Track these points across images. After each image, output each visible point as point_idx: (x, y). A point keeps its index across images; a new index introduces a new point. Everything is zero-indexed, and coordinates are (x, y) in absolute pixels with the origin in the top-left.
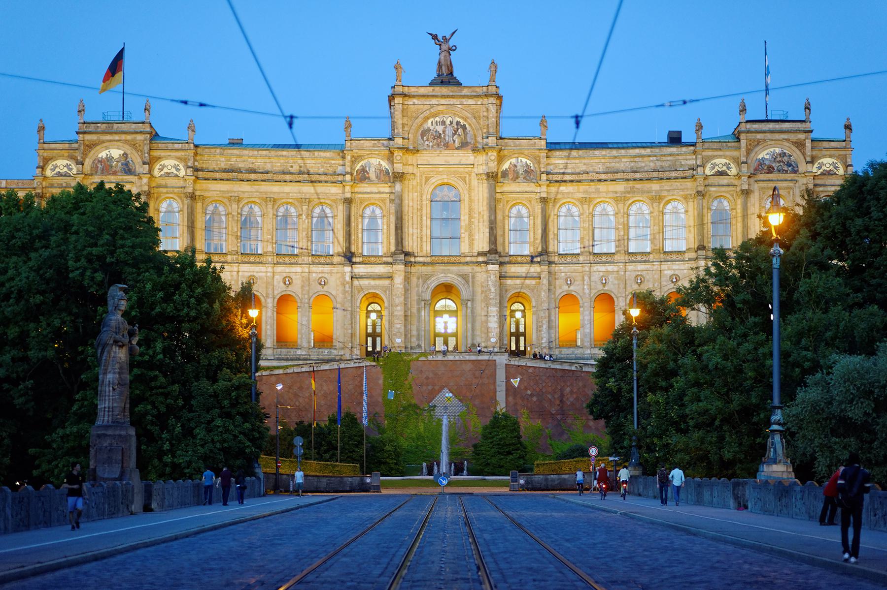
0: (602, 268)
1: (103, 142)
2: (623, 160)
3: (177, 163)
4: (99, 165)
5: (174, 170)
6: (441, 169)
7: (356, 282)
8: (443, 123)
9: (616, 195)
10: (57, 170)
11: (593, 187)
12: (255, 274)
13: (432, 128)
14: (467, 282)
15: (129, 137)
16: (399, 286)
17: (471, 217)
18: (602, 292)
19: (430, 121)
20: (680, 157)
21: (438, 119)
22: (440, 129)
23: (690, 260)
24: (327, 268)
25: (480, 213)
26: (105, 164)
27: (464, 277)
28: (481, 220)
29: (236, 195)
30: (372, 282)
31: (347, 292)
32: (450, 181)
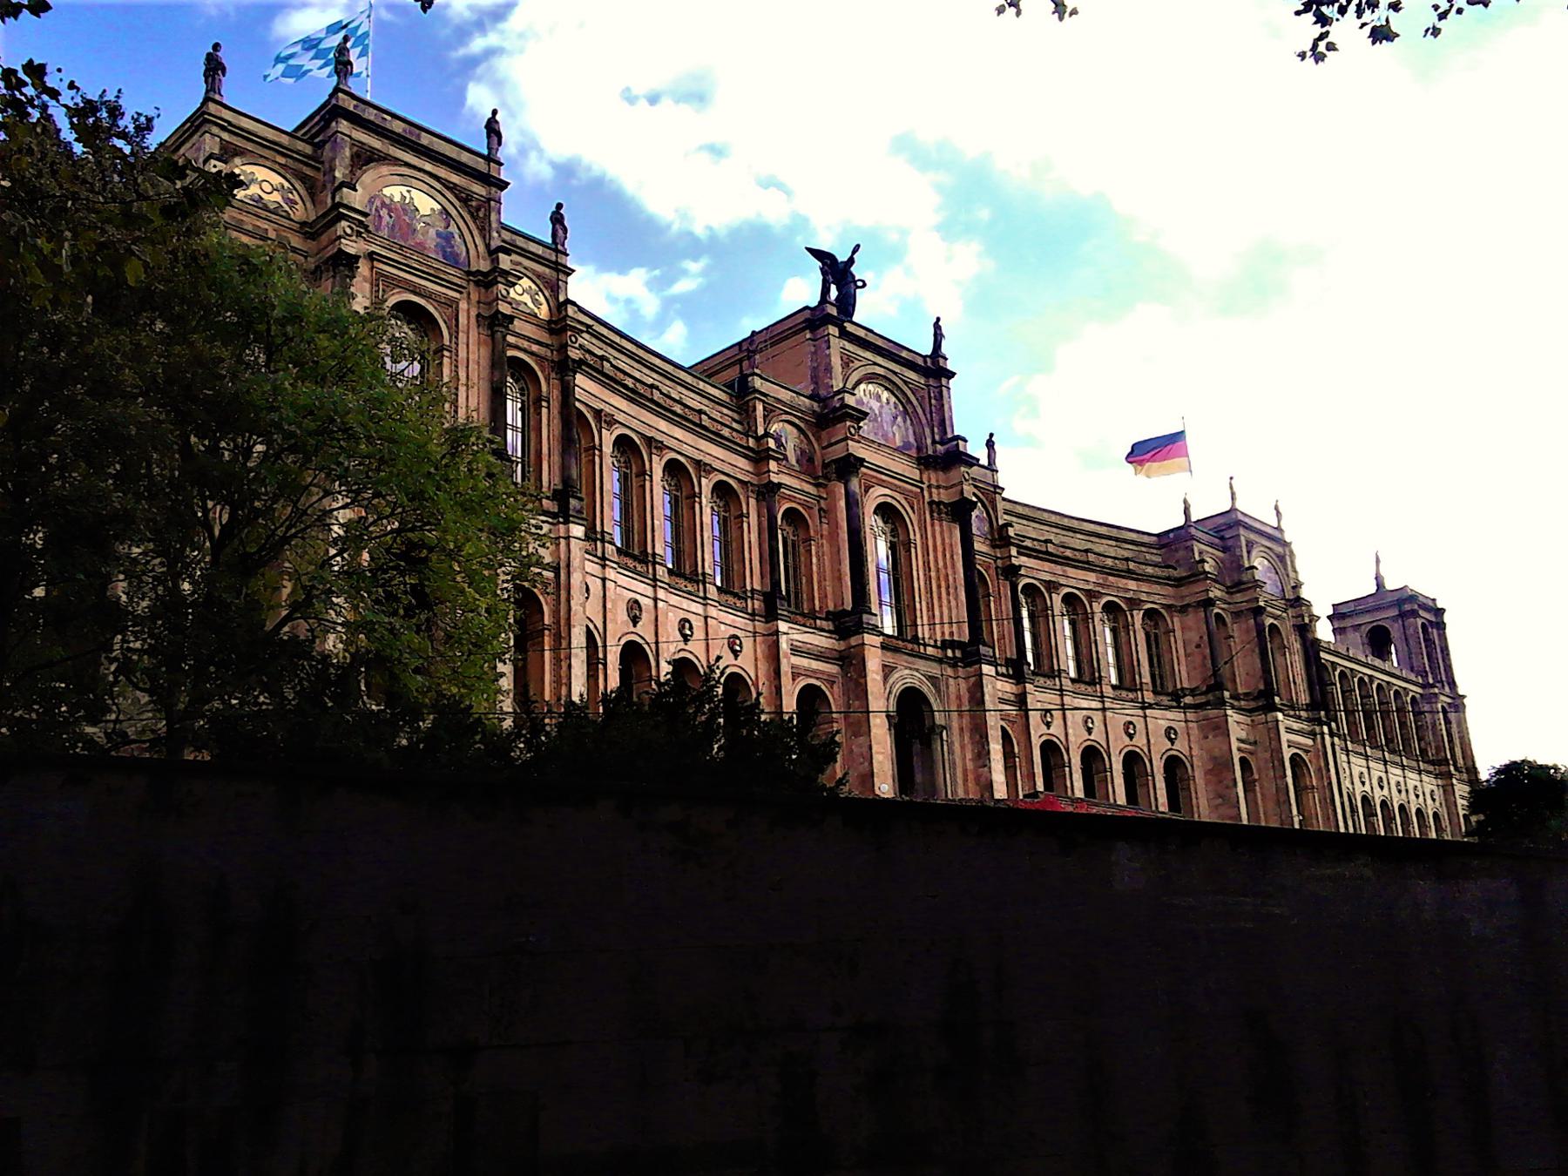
0: (1085, 704)
1: (396, 161)
2: (1079, 536)
3: (534, 287)
4: (384, 212)
5: (526, 298)
6: (883, 477)
7: (796, 660)
8: (878, 398)
9: (1090, 587)
10: (254, 190)
11: (1058, 569)
12: (638, 597)
13: (865, 400)
14: (938, 690)
15: (455, 178)
16: (875, 676)
17: (928, 579)
18: (1089, 743)
19: (862, 386)
20: (1143, 549)
21: (871, 387)
22: (875, 405)
23: (1187, 707)
24: (740, 622)
25: (938, 570)
26: (399, 217)
27: (932, 679)
28: (943, 584)
29: (607, 409)
30: (815, 665)
31: (787, 672)
32: (895, 503)
